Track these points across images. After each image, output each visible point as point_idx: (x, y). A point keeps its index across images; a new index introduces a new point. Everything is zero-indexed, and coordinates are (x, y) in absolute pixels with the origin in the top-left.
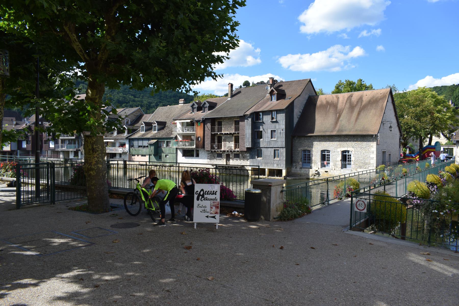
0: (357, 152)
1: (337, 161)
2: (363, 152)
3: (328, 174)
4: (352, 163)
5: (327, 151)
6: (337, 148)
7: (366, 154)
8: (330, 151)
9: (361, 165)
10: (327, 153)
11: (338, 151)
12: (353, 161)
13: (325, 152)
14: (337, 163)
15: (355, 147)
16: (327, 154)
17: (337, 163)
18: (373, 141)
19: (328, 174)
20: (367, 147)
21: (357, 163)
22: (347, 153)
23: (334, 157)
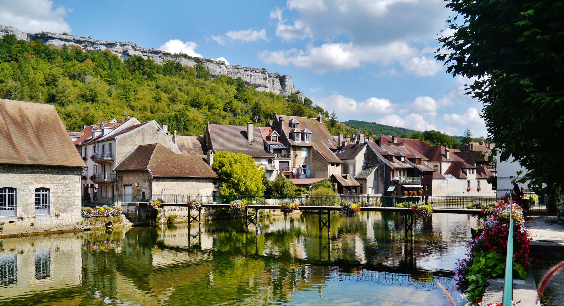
0: (57, 190)
1: (28, 204)
2: (66, 190)
3: (15, 225)
4: (52, 205)
5: (9, 188)
6: (28, 184)
7: (69, 192)
8: (15, 189)
9: (63, 207)
10: (9, 192)
11: (30, 188)
12: (52, 203)
13: (5, 192)
14: (29, 207)
15: (55, 184)
16: (10, 193)
17: (29, 207)
18: (78, 175)
19: (15, 225)
20: (71, 183)
21: (58, 205)
22: (41, 191)
23: (23, 198)
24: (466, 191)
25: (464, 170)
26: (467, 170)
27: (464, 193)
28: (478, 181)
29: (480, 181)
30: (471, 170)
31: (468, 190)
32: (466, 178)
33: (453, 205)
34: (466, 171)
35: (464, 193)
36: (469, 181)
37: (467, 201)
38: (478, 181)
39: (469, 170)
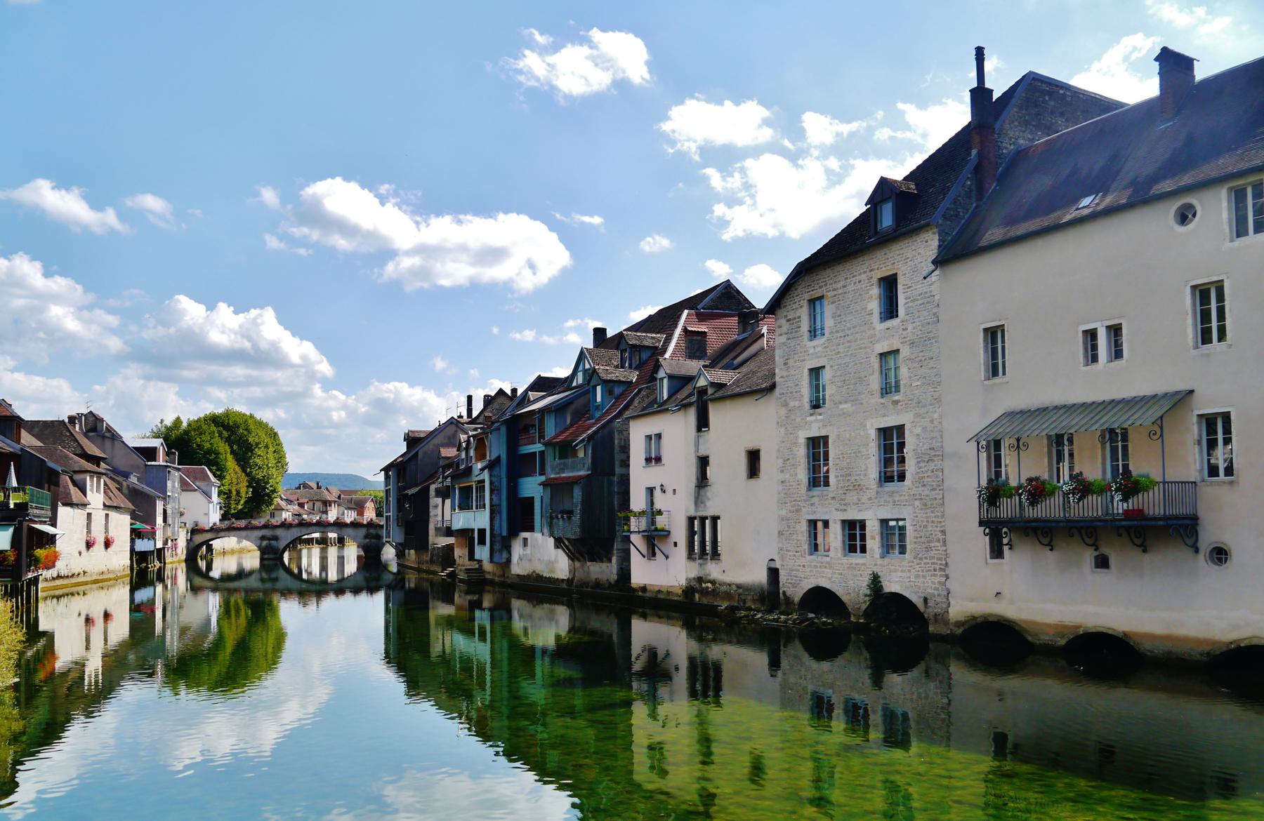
24: (83, 547)
25: (77, 477)
26: (88, 478)
27: (80, 553)
28: (107, 515)
29: (110, 513)
30: (95, 479)
31: (89, 545)
32: (84, 505)
33: (58, 597)
34: (85, 480)
35: (80, 553)
36: (89, 515)
37: (86, 583)
38: (107, 515)
39: (92, 477)
